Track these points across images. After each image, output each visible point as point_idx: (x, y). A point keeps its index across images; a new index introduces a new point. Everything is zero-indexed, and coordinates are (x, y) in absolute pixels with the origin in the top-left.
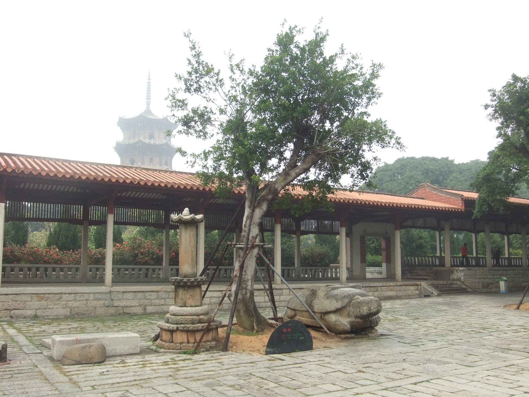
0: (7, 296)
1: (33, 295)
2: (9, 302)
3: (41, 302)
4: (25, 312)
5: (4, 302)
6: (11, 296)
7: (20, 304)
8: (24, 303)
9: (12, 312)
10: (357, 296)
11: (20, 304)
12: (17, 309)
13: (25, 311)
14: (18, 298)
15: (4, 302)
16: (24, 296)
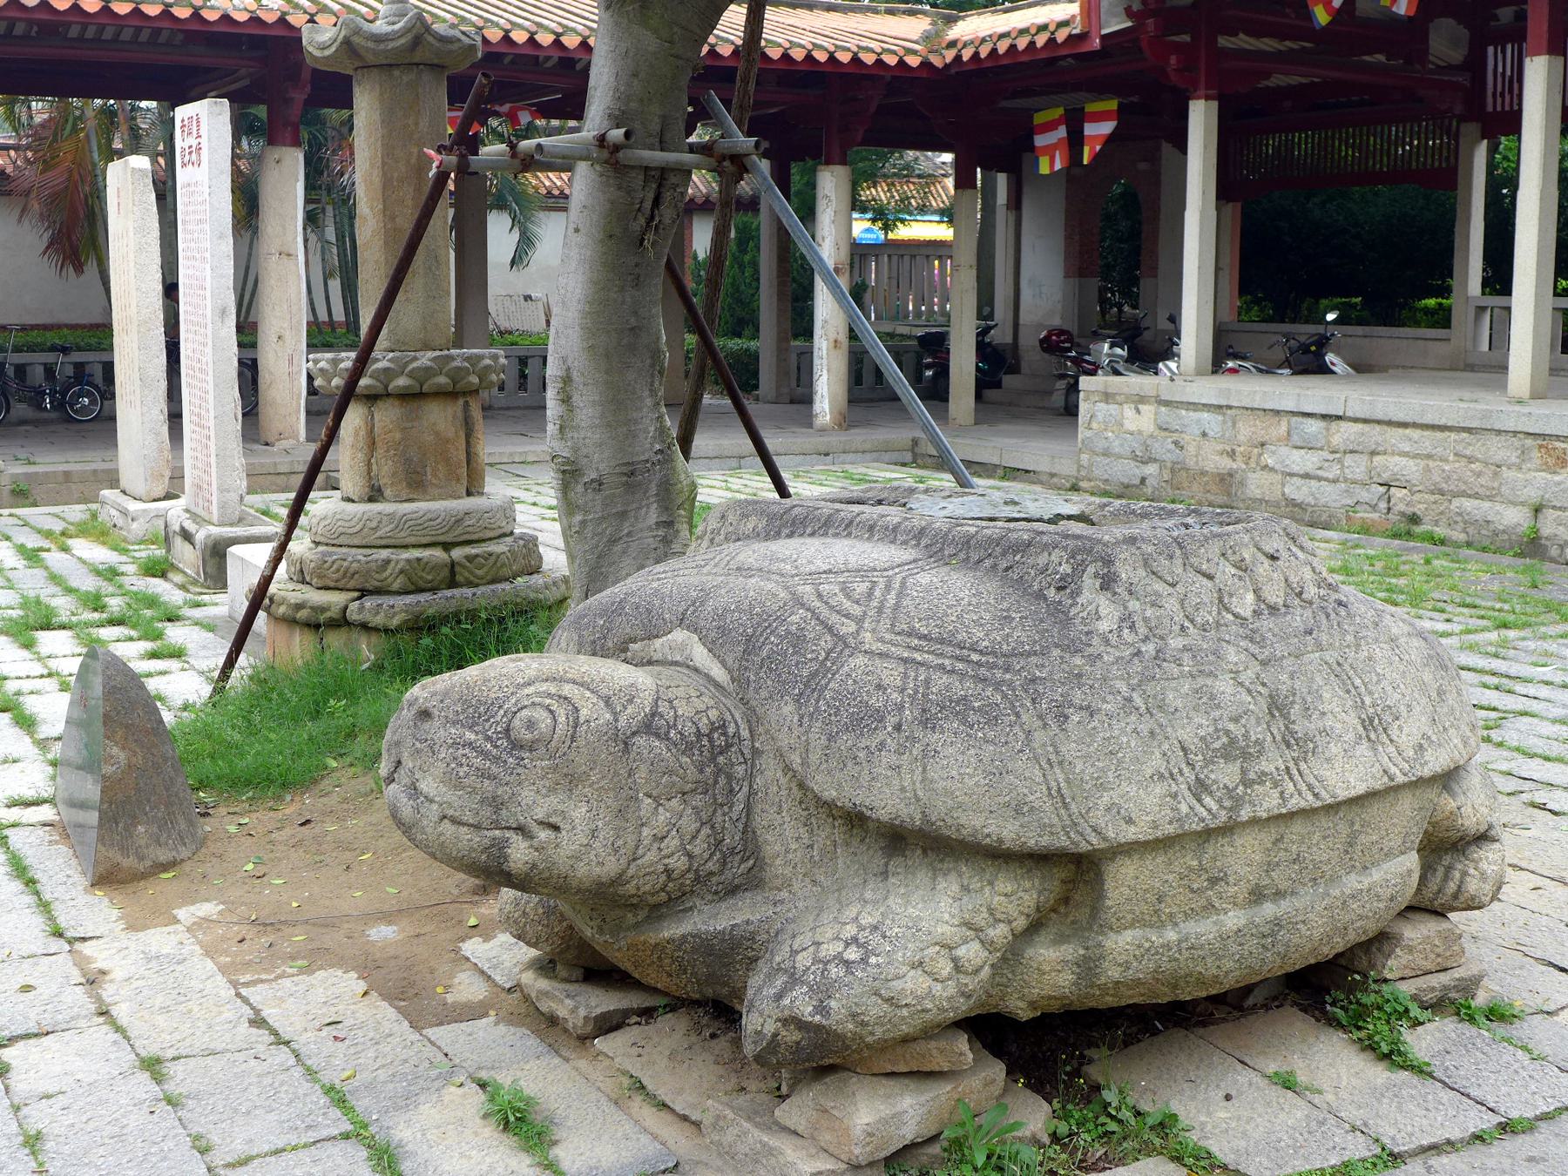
0: (1439, 435)
1: (1529, 442)
2: (1446, 461)
3: (1557, 478)
4: (1498, 513)
5: (1429, 456)
6: (1453, 436)
7: (1479, 475)
8: (1496, 474)
9: (1456, 502)
10: (679, 635)
11: (1479, 475)
12: (1470, 496)
13: (1498, 507)
14: (1476, 447)
15: (1429, 456)
16: (1496, 439)
